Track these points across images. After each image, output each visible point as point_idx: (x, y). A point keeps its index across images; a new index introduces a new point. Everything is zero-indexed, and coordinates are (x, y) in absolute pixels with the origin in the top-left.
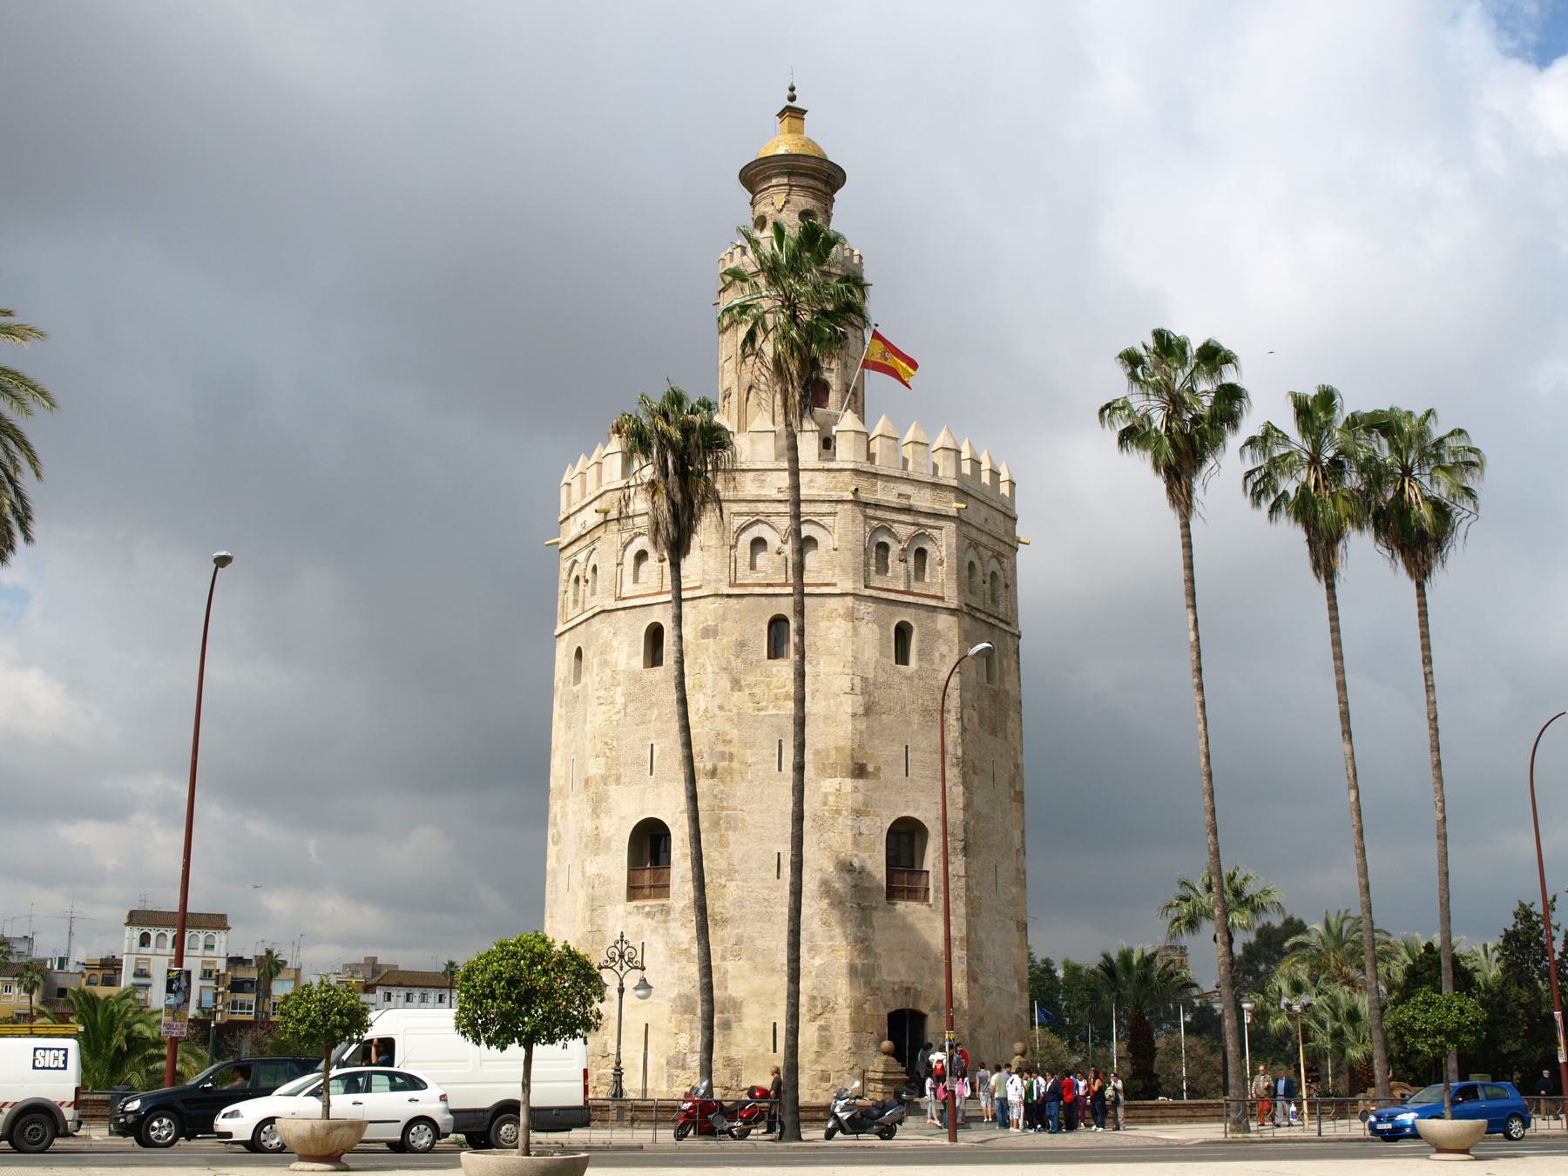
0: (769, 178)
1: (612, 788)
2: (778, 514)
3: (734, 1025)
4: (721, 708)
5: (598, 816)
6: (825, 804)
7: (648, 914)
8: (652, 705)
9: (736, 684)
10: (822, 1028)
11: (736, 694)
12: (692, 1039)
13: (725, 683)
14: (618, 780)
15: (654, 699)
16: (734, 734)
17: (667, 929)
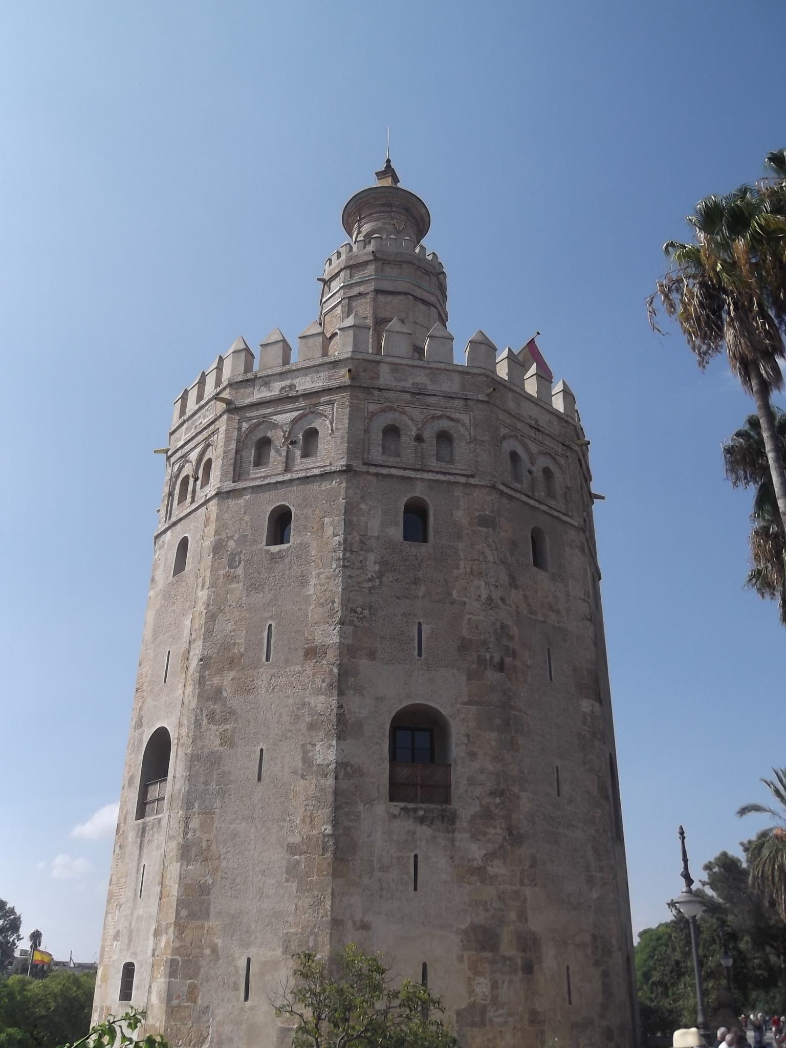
1: (364, 663)
2: (530, 438)
3: (536, 967)
4: (502, 599)
6: (585, 723)
7: (422, 820)
8: (416, 581)
9: (513, 583)
10: (605, 975)
11: (513, 591)
12: (495, 986)
13: (504, 577)
14: (372, 655)
15: (420, 574)
16: (514, 631)
17: (453, 841)
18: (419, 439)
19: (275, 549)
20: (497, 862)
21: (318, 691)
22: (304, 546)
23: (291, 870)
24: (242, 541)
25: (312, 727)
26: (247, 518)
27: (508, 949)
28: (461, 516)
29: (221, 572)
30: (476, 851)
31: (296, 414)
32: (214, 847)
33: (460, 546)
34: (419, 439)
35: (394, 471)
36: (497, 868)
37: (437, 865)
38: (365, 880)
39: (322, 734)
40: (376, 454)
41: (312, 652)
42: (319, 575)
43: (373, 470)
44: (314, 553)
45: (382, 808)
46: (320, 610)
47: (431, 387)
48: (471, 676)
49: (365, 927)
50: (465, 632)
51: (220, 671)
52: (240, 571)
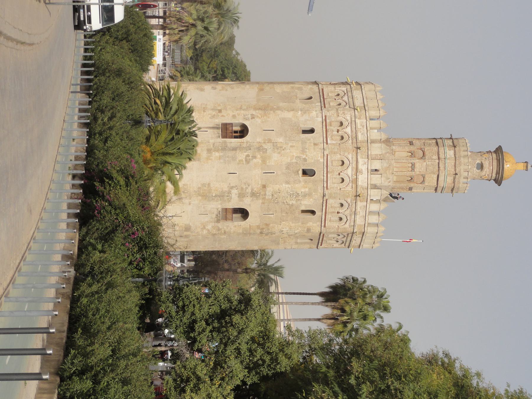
0: (496, 174)
1: (261, 201)
2: (347, 239)
5: (251, 197)
7: (217, 215)
14: (263, 203)
18: (338, 213)
19: (301, 172)
20: (207, 232)
21: (252, 190)
22: (300, 182)
23: (204, 185)
24: (305, 160)
25: (242, 188)
26: (313, 161)
27: (186, 233)
28: (310, 224)
29: (294, 154)
30: (209, 227)
31: (350, 175)
32: (210, 161)
33: (300, 224)
34: (338, 213)
35: (324, 207)
36: (205, 232)
37: (205, 219)
38: (201, 204)
39: (240, 192)
40: (330, 201)
41: (264, 187)
42: (289, 188)
43: (324, 202)
44: (297, 185)
45: (220, 207)
46: (277, 189)
47: (358, 217)
48: (258, 227)
49: (190, 204)
50: (271, 225)
51: (262, 157)
52: (294, 161)
